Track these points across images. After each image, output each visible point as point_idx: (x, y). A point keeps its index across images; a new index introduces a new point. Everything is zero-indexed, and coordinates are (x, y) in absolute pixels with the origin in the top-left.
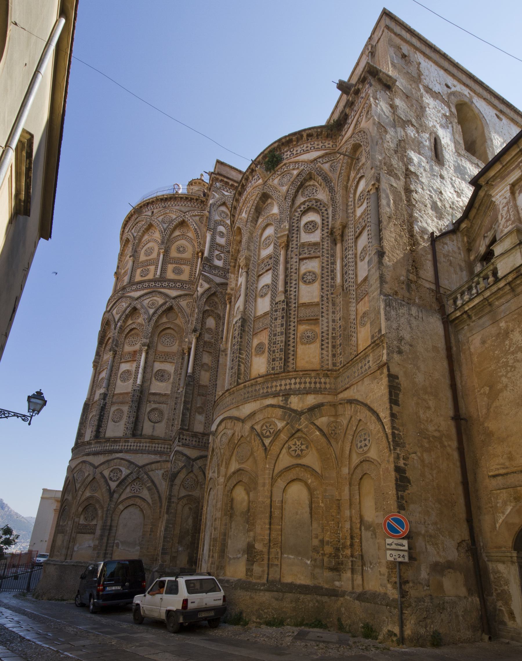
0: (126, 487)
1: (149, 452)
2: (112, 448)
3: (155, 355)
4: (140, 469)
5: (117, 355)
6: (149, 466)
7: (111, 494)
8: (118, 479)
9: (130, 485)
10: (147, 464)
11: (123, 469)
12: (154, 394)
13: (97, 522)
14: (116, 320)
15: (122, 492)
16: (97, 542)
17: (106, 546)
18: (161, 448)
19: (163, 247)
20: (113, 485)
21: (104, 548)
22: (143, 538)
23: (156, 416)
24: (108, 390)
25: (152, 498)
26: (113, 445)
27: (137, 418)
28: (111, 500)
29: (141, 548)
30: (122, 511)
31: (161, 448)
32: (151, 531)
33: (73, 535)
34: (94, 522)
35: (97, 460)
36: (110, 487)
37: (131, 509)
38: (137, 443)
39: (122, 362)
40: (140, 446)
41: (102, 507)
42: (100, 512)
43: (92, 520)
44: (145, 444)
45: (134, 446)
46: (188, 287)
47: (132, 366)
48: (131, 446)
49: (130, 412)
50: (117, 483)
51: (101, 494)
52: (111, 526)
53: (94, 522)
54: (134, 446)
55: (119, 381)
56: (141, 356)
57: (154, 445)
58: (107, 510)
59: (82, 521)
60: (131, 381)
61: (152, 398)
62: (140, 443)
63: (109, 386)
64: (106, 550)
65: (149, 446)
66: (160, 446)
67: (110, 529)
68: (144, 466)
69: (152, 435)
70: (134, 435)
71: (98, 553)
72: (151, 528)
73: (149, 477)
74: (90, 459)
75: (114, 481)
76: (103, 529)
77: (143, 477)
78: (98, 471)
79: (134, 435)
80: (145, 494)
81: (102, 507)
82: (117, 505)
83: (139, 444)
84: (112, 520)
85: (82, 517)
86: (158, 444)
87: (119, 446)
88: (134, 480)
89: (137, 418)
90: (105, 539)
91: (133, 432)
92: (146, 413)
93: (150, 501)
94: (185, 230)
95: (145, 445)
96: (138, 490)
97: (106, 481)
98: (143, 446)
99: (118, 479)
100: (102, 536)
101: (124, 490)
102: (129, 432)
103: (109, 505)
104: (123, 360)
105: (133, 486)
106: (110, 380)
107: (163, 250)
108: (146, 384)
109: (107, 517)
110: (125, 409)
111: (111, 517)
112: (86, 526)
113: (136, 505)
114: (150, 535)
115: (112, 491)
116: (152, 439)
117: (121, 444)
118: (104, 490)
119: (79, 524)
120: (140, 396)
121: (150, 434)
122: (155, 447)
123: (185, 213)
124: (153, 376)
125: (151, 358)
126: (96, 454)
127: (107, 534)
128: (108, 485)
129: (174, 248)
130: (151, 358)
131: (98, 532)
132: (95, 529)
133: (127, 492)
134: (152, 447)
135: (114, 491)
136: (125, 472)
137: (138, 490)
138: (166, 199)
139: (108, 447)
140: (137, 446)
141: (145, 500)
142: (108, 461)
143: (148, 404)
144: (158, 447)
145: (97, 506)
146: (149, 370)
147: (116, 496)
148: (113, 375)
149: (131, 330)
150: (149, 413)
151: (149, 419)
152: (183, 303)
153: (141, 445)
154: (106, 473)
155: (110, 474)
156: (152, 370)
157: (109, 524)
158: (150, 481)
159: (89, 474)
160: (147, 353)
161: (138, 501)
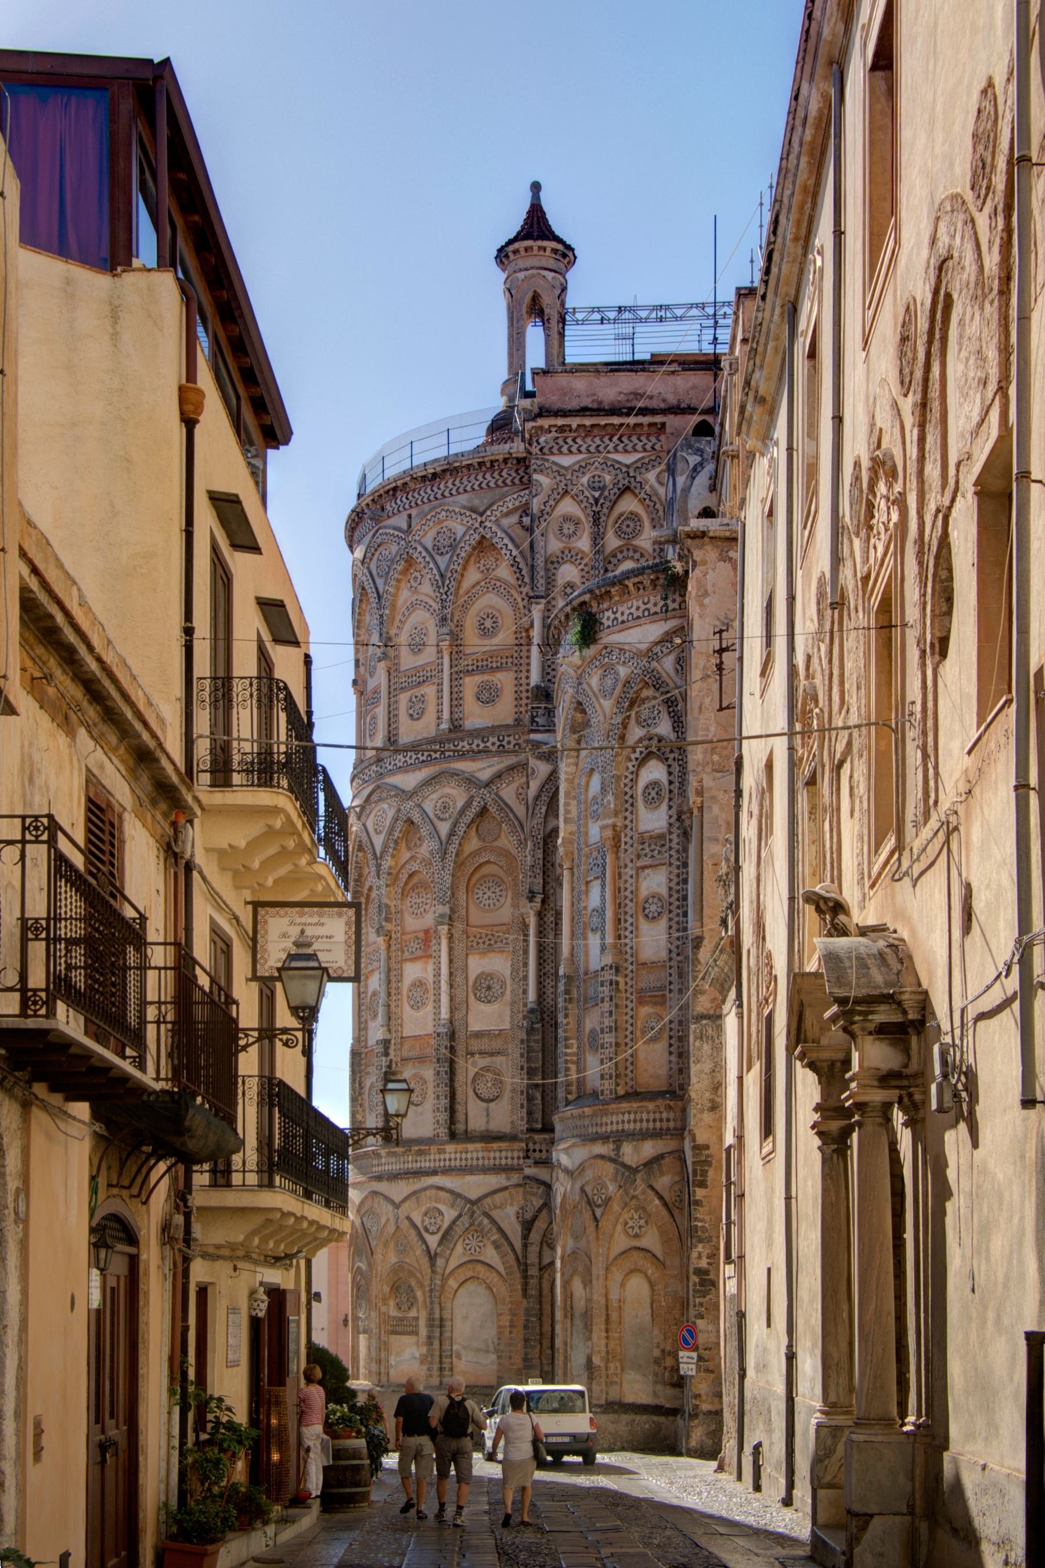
0: (455, 1245)
1: (485, 1170)
2: (418, 1165)
3: (468, 937)
4: (475, 1208)
5: (392, 942)
6: (489, 1200)
7: (432, 1258)
8: (438, 1230)
9: (461, 1239)
10: (486, 1196)
11: (442, 1208)
12: (479, 1035)
13: (418, 1311)
14: (378, 850)
15: (450, 1255)
16: (424, 1350)
17: (441, 1356)
18: (506, 1158)
19: (445, 630)
20: (433, 1241)
21: (437, 1359)
22: (499, 1339)
23: (489, 1084)
24: (389, 1030)
25: (503, 1263)
26: (419, 1159)
27: (453, 1096)
28: (433, 1272)
29: (499, 1357)
30: (456, 1291)
31: (506, 1158)
32: (511, 1326)
33: (384, 1337)
34: (413, 1313)
35: (398, 1190)
36: (427, 1247)
37: (471, 1286)
38: (461, 1153)
39: (406, 960)
40: (466, 1159)
41: (422, 1286)
42: (419, 1294)
43: (409, 1308)
44: (475, 1152)
45: (456, 1159)
46: (513, 742)
47: (426, 970)
48: (450, 1160)
49: (438, 1084)
50: (438, 1237)
51: (417, 1257)
52: (441, 1319)
53: (413, 1313)
54: (456, 1159)
55: (407, 1008)
56: (439, 944)
57: (492, 1155)
58: (431, 1291)
59: (393, 1312)
60: (430, 1008)
61: (475, 1045)
62: (466, 1152)
63: (389, 1019)
64: (441, 1362)
65: (483, 1158)
66: (504, 1154)
67: (441, 1326)
68: (480, 1199)
69: (487, 1130)
70: (453, 1136)
71: (429, 1369)
72: (511, 1321)
73: (493, 1221)
74: (382, 1187)
75: (433, 1233)
76: (430, 1325)
77: (481, 1223)
78: (403, 1210)
79: (453, 1136)
80: (491, 1255)
81: (422, 1286)
82: (445, 1279)
83: (464, 1156)
84: (441, 1309)
85: (392, 1303)
86: (500, 1151)
87: (430, 1161)
88: (467, 1229)
89: (453, 1096)
90: (436, 1343)
91: (450, 1129)
92: (470, 1081)
93: (502, 1270)
94: (490, 561)
95: (475, 1155)
96: (478, 1249)
97: (420, 1234)
98: (472, 1159)
99: (438, 1230)
100: (430, 1338)
101: (452, 1250)
102: (443, 1131)
103: (431, 1280)
104: (407, 955)
105: (467, 1241)
106: (389, 1006)
107: (447, 643)
108: (458, 1015)
109: (432, 1303)
110: (428, 1073)
111: (440, 1304)
112: (401, 1319)
113: (478, 1278)
114: (511, 1332)
115: (432, 1253)
116: (489, 1137)
117: (432, 1157)
118: (418, 1252)
119: (389, 1317)
120: (452, 1046)
121: (483, 1128)
122: (495, 1158)
123: (481, 515)
124: (470, 990)
125: (460, 947)
126: (393, 1177)
127: (437, 1334)
128: (424, 1242)
129: (470, 623)
130: (460, 947)
131: (423, 1331)
132: (417, 1326)
133: (458, 1254)
134: (489, 1159)
135: (436, 1254)
136: (449, 1214)
137: (478, 1249)
138: (435, 475)
139: (410, 1162)
140: (461, 1159)
141: (493, 1268)
142: (414, 1193)
143: (470, 1061)
144: (501, 1158)
145: (413, 1283)
146: (459, 979)
147: (440, 1262)
148: (393, 992)
149: (411, 876)
150: (474, 1080)
151: (476, 1094)
152: (508, 792)
153: (469, 1156)
154: (417, 1219)
155: (423, 1221)
156: (467, 978)
157: (437, 1316)
158: (495, 1231)
159: (388, 1220)
160: (451, 937)
161: (481, 1270)
